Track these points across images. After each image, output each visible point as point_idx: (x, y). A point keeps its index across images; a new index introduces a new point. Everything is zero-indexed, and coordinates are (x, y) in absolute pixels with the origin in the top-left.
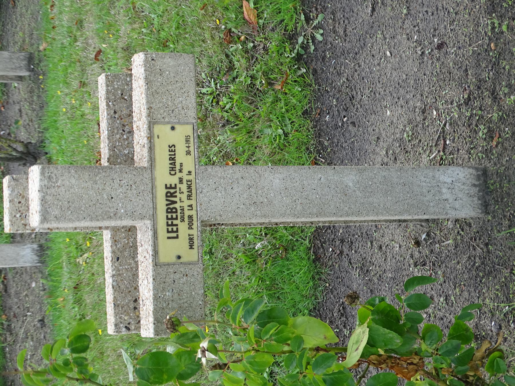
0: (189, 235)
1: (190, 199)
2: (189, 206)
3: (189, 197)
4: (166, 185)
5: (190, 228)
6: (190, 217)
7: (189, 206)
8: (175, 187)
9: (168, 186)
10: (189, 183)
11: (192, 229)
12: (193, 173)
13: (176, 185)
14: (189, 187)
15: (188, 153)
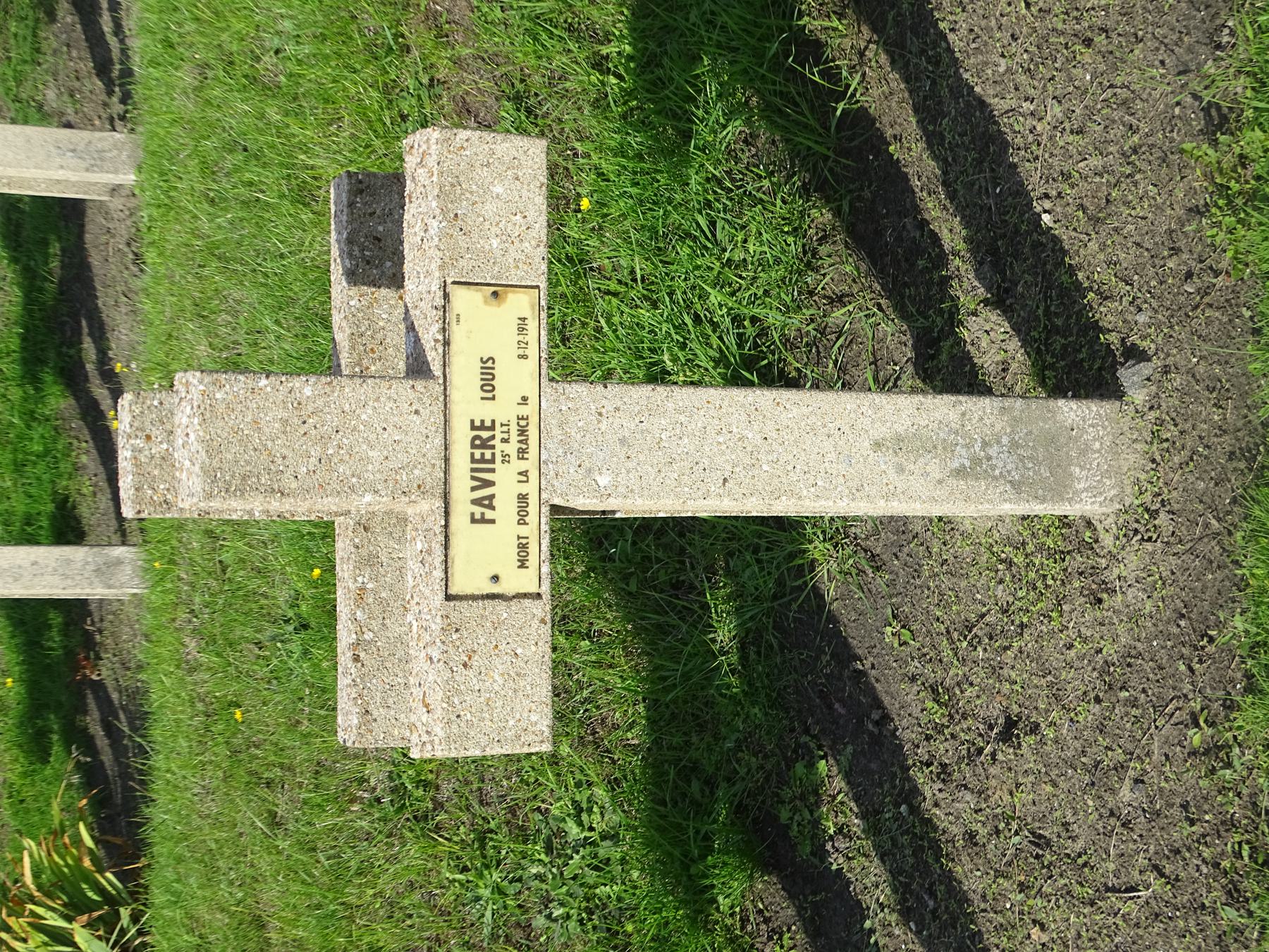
0: (519, 538)
1: (523, 458)
2: (520, 474)
3: (522, 454)
4: (472, 422)
5: (522, 522)
6: (523, 498)
7: (520, 474)
8: (492, 428)
9: (477, 423)
10: (523, 423)
11: (526, 524)
12: (533, 400)
13: (493, 422)
14: (522, 432)
15: (524, 357)
